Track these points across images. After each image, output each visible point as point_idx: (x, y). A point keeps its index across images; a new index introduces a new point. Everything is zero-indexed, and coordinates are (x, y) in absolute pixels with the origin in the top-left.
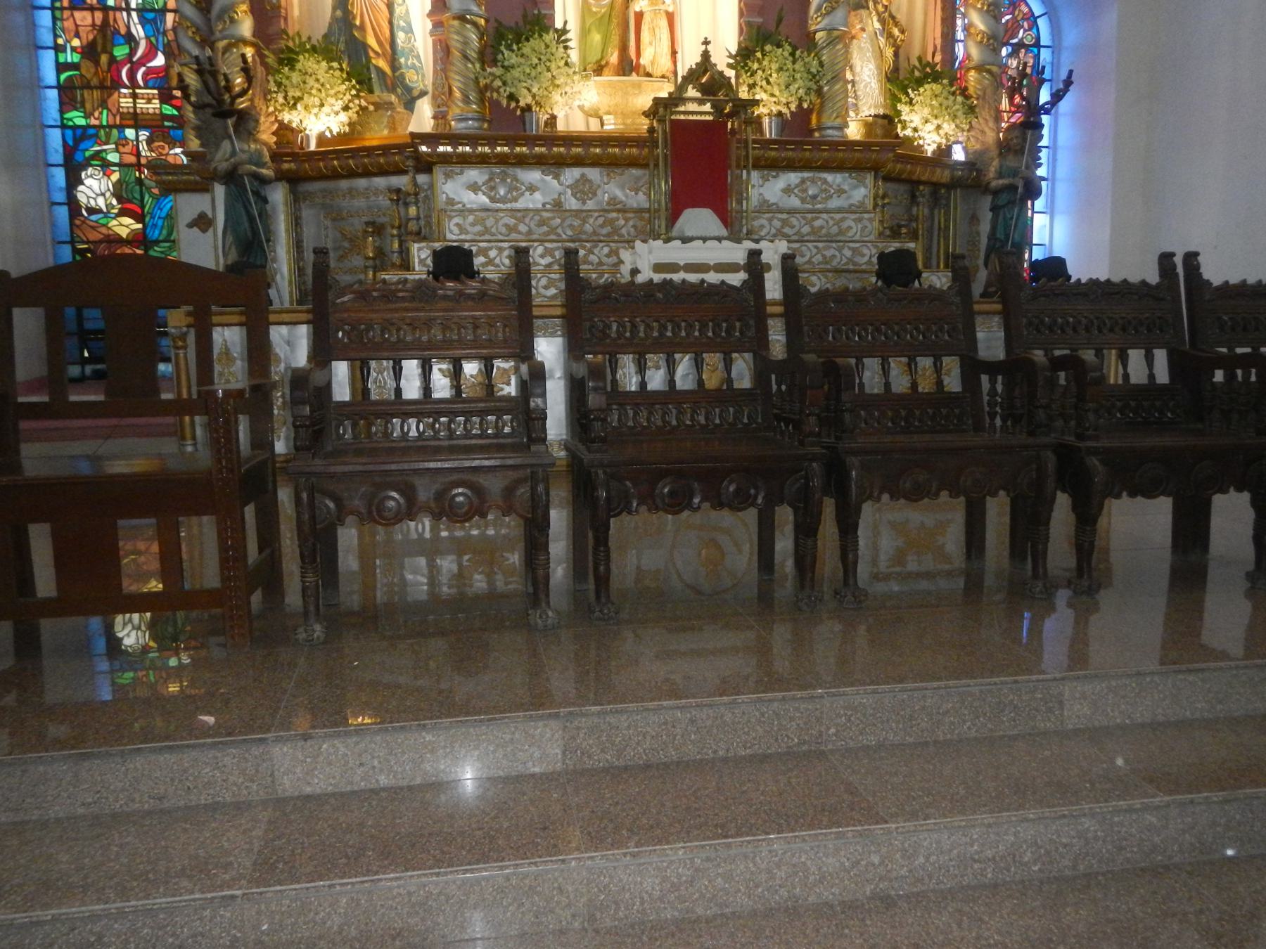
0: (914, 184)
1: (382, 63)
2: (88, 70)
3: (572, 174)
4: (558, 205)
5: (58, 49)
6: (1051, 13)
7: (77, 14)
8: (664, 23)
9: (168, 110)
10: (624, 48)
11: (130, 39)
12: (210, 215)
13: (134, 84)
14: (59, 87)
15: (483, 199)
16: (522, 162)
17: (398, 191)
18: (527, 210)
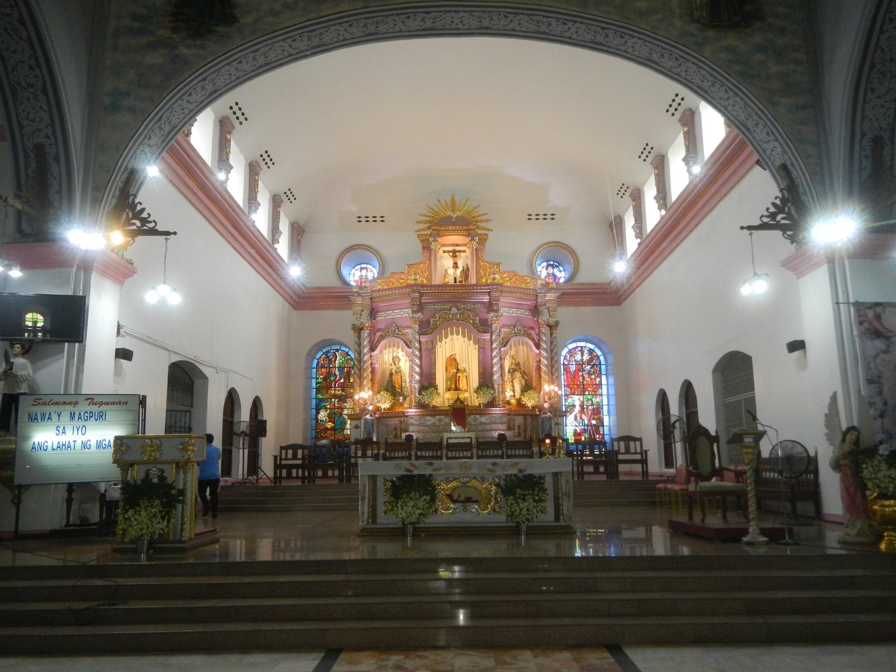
0: (525, 415)
1: (399, 390)
2: (324, 384)
3: (438, 417)
4: (434, 423)
5: (317, 378)
6: (604, 354)
7: (323, 369)
8: (465, 378)
9: (343, 393)
10: (456, 385)
11: (335, 375)
12: (359, 425)
13: (335, 387)
14: (316, 388)
15: (418, 423)
16: (427, 415)
17: (401, 421)
18: (427, 425)
